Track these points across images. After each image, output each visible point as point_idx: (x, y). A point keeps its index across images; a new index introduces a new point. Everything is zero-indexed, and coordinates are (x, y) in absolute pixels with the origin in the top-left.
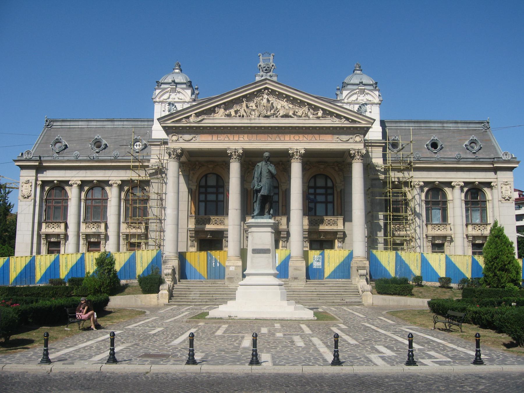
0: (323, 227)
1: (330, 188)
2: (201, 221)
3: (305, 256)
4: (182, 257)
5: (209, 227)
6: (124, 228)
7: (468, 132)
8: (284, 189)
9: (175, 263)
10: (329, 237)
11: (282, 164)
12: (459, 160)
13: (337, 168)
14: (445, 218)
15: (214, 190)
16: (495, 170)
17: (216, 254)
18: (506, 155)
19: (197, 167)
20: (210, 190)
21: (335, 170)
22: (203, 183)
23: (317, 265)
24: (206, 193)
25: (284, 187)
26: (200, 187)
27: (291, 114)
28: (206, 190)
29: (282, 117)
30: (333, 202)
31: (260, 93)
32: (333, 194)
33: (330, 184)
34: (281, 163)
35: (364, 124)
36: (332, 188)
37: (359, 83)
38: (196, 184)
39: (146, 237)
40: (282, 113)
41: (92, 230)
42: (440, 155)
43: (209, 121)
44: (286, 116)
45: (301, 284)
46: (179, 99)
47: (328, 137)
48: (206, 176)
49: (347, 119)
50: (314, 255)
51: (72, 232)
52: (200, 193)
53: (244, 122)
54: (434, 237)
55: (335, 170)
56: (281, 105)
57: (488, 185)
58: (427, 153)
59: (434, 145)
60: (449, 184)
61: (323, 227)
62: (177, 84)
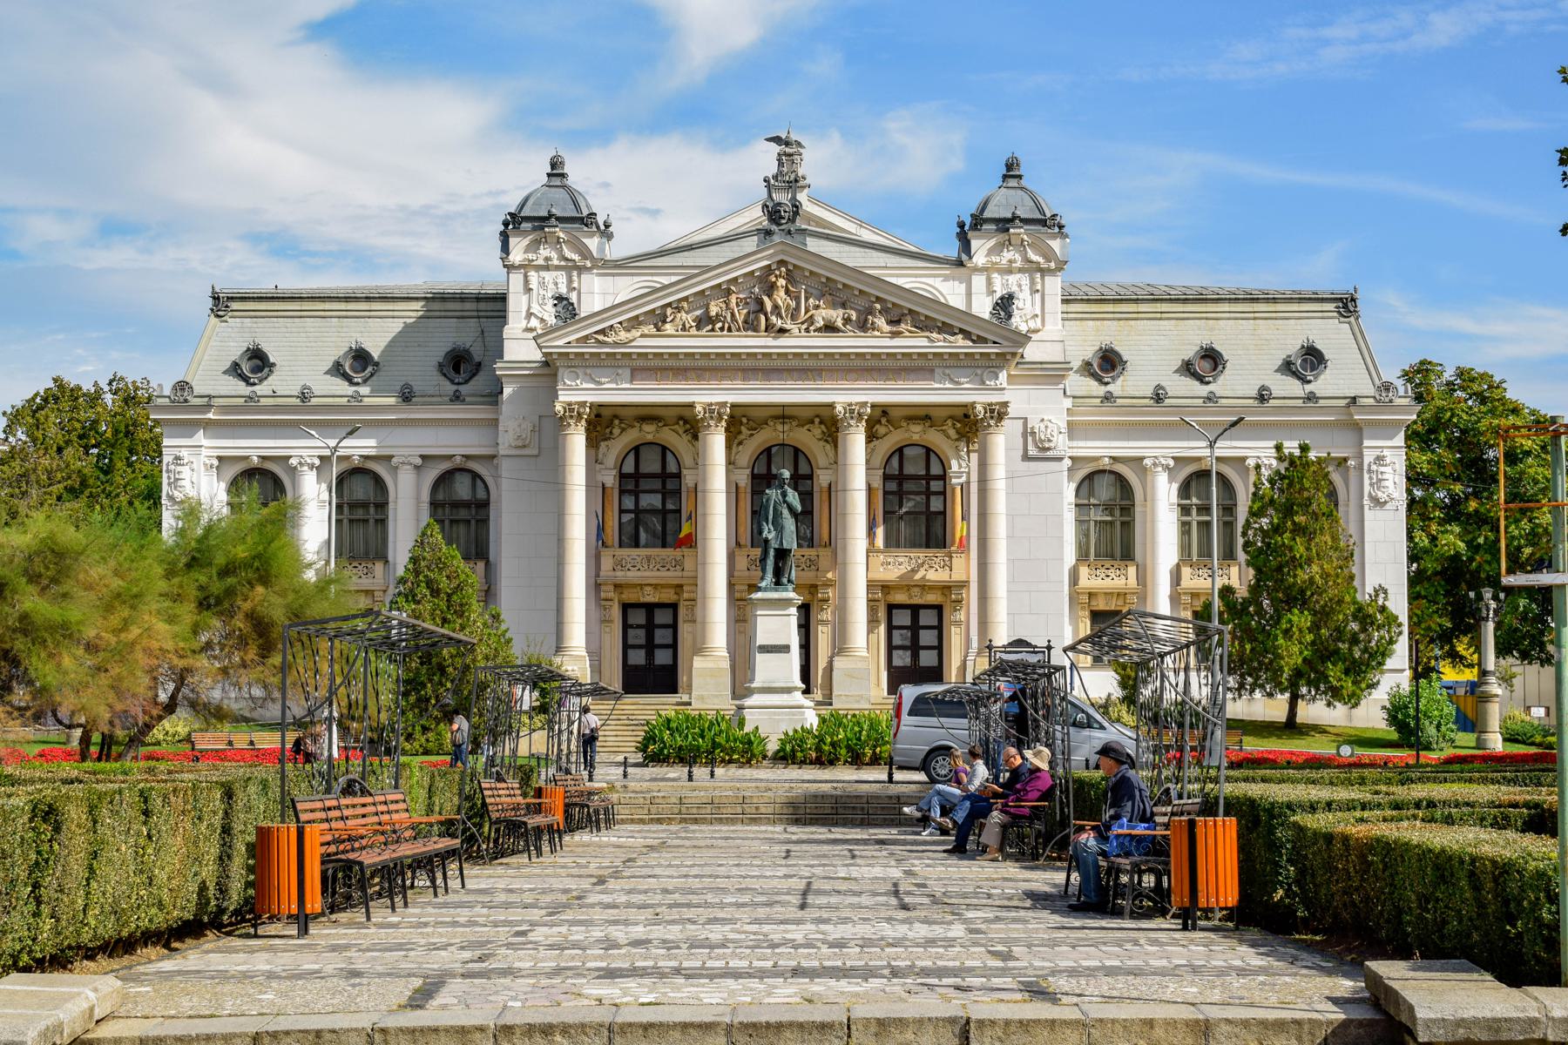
1: (937, 478)
8: (825, 484)
10: (931, 598)
11: (821, 423)
13: (952, 432)
15: (657, 484)
18: (1387, 390)
19: (616, 431)
20: (644, 484)
21: (948, 437)
22: (629, 467)
24: (636, 494)
25: (823, 478)
26: (622, 476)
27: (839, 323)
28: (637, 485)
29: (818, 330)
30: (944, 513)
32: (944, 493)
33: (936, 469)
34: (817, 420)
36: (943, 477)
37: (1009, 216)
38: (614, 472)
40: (820, 323)
44: (830, 328)
46: (567, 259)
48: (636, 450)
49: (967, 335)
52: (622, 492)
55: (948, 437)
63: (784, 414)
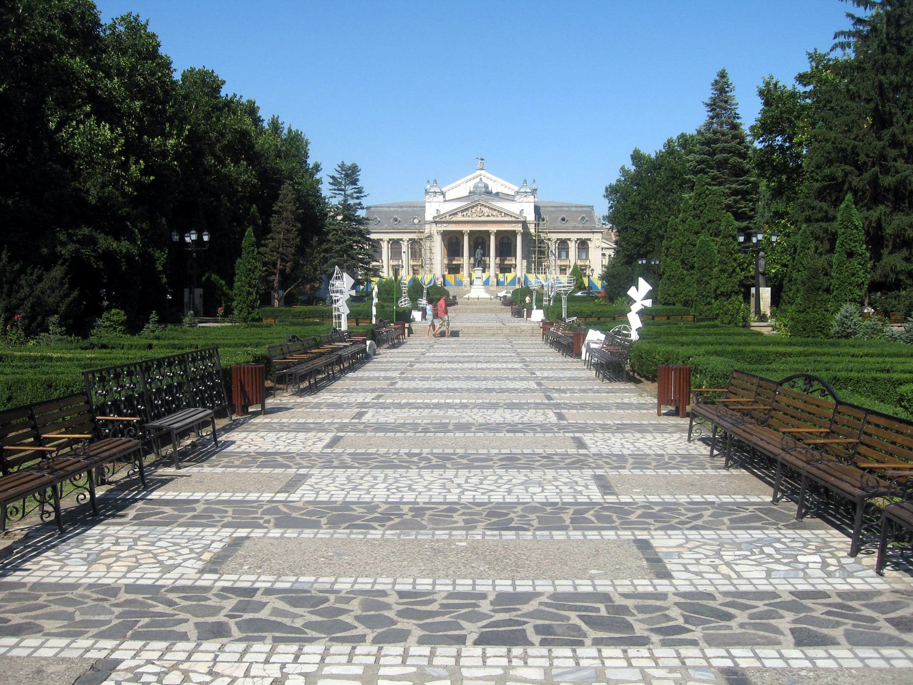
0: (506, 262)
2: (450, 260)
3: (497, 276)
4: (444, 276)
5: (454, 262)
6: (411, 263)
7: (581, 212)
9: (442, 279)
12: (575, 227)
14: (567, 256)
16: (593, 233)
17: (457, 275)
23: (502, 280)
31: (477, 205)
35: (522, 219)
39: (422, 267)
41: (395, 263)
42: (567, 225)
43: (454, 219)
44: (488, 216)
45: (494, 288)
47: (507, 225)
50: (501, 276)
51: (385, 264)
53: (470, 219)
54: (561, 266)
56: (486, 210)
57: (589, 240)
58: (559, 224)
59: (563, 219)
60: (569, 239)
61: (506, 262)
62: (436, 192)
63: (480, 231)
